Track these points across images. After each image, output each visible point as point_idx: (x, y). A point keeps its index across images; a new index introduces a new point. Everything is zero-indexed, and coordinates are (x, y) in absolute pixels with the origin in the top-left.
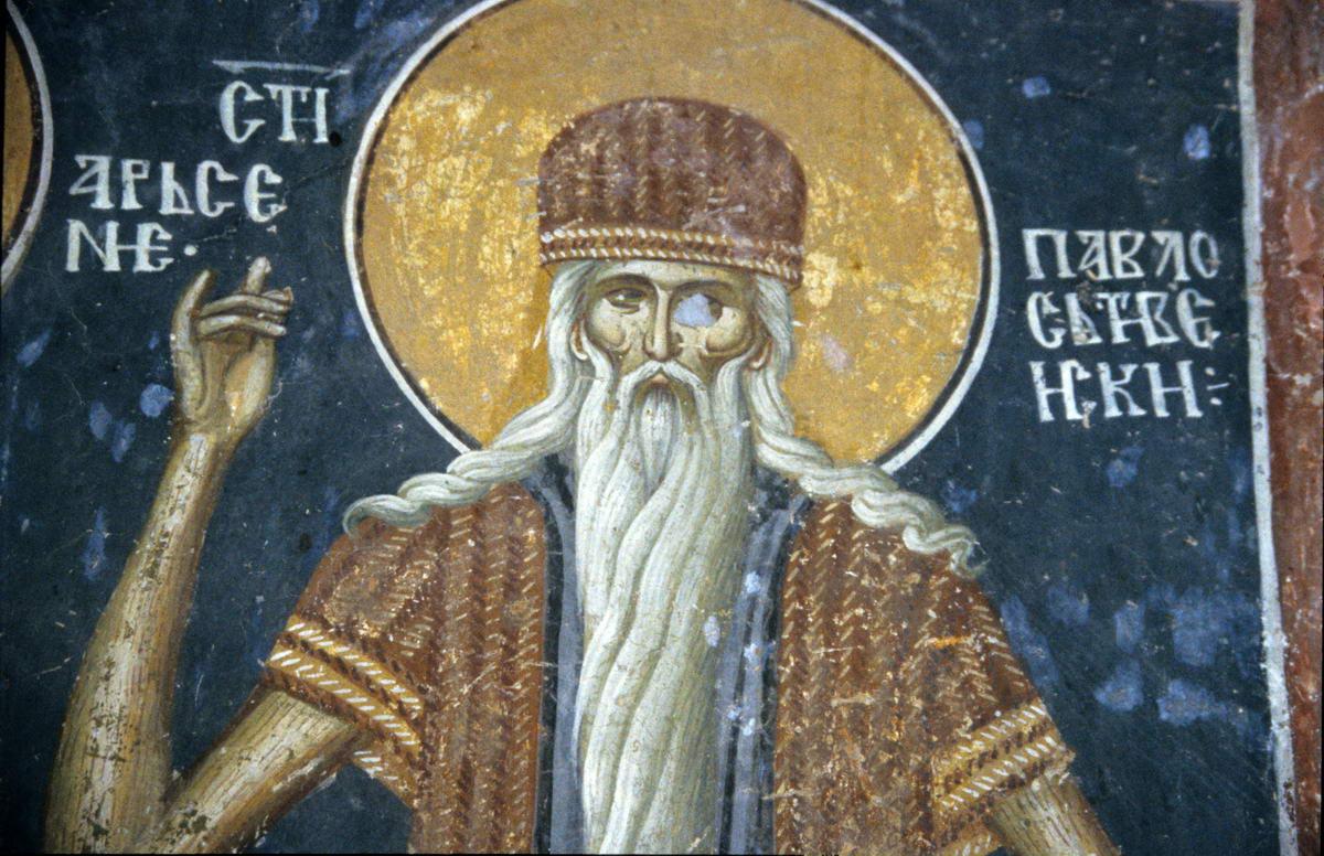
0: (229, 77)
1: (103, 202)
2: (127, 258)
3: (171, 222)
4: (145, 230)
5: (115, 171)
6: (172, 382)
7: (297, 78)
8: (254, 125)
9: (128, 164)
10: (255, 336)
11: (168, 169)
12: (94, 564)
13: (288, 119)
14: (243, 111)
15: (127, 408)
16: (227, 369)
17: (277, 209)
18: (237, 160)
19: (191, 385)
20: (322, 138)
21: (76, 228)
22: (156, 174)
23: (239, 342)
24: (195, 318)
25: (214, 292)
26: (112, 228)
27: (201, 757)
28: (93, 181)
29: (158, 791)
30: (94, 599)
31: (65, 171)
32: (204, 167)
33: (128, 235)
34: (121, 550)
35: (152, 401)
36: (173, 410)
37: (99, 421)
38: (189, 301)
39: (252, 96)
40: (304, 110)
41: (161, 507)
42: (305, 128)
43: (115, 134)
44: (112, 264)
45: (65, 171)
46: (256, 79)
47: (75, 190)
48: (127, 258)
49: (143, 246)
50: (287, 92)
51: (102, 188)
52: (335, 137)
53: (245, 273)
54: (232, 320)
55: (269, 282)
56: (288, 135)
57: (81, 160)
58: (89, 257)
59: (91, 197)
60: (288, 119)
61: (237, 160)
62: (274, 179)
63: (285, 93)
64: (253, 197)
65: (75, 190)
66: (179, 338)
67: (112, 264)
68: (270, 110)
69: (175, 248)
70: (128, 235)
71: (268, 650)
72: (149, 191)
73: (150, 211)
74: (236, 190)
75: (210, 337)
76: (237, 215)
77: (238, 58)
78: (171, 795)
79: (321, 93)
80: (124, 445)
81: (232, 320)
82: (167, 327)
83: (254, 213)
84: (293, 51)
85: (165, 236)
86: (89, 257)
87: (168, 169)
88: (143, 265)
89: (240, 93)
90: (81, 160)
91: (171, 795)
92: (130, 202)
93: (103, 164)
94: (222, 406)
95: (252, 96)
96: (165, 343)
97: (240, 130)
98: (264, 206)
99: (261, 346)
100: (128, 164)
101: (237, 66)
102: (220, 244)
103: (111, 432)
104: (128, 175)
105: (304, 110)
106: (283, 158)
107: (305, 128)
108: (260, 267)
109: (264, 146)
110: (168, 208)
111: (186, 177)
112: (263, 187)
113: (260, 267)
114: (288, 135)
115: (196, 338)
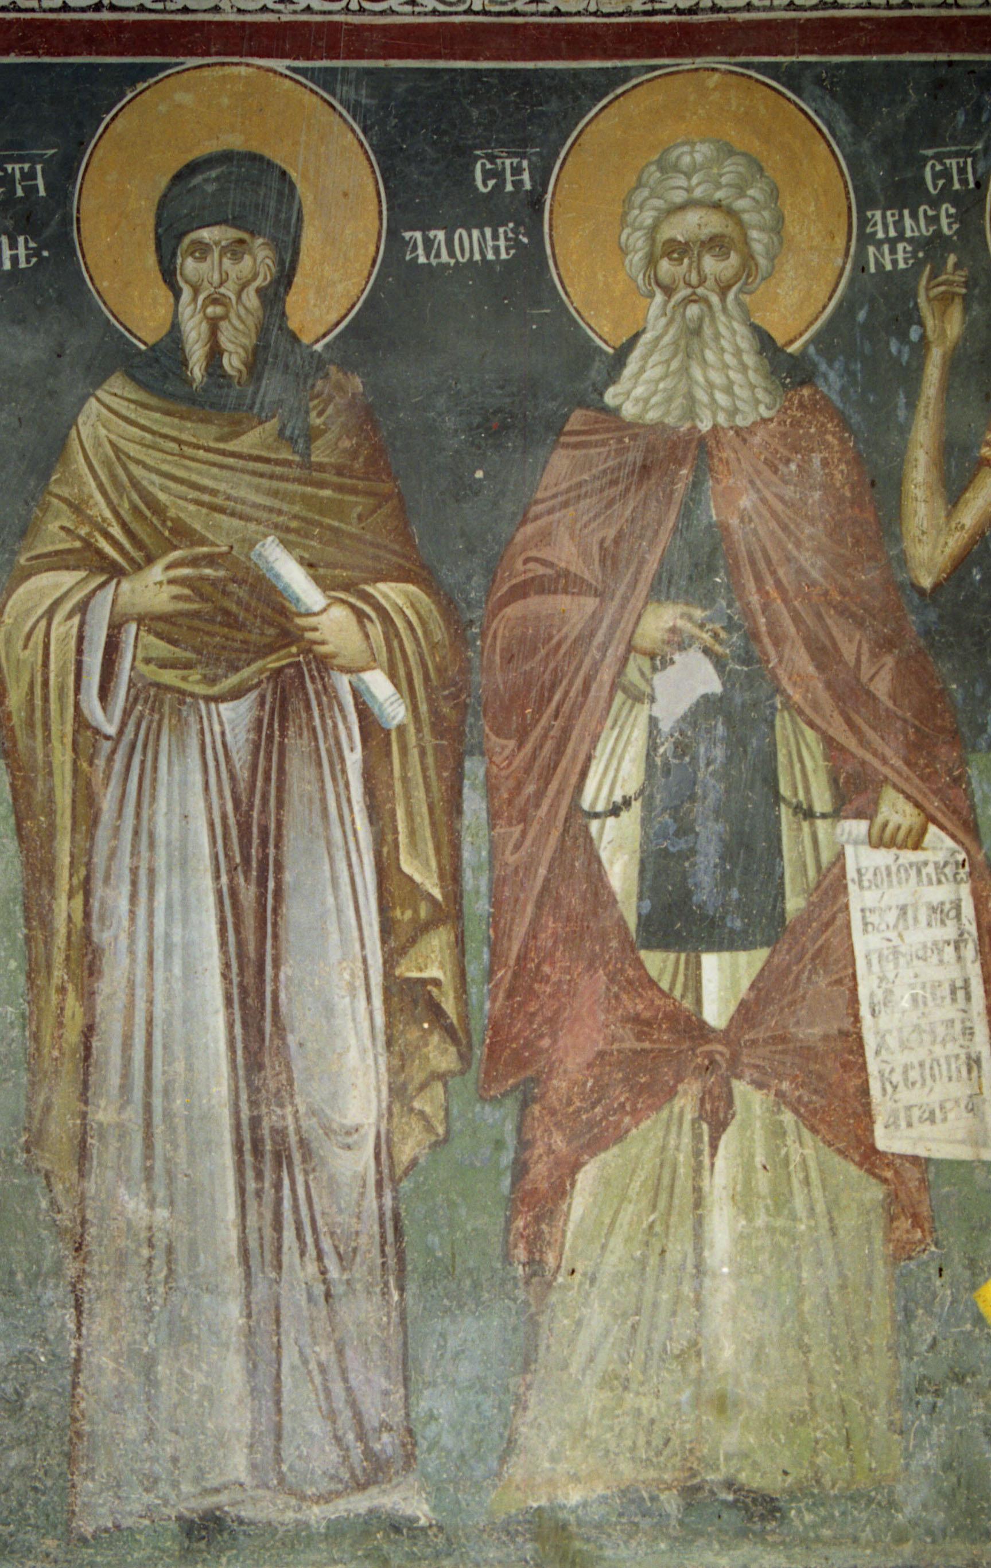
0: (926, 159)
1: (880, 235)
2: (895, 262)
3: (911, 241)
4: (900, 246)
5: (884, 217)
6: (921, 324)
7: (957, 154)
8: (941, 182)
9: (889, 213)
10: (954, 294)
11: (906, 212)
12: (902, 414)
13: (956, 177)
14: (936, 176)
15: (903, 337)
16: (944, 313)
17: (955, 227)
18: (935, 204)
19: (930, 323)
20: (972, 185)
21: (871, 249)
22: (901, 216)
23: (947, 299)
24: (928, 289)
25: (934, 275)
26: (886, 248)
27: (959, 498)
28: (875, 224)
29: (943, 514)
30: (905, 430)
31: (864, 221)
32: (921, 209)
33: (893, 251)
34: (912, 405)
35: (914, 333)
36: (923, 337)
37: (894, 348)
38: (923, 282)
39: (938, 168)
40: (962, 171)
41: (926, 385)
42: (964, 182)
43: (882, 198)
44: (889, 267)
45: (864, 221)
46: (939, 157)
47: (869, 230)
48: (895, 262)
49: (900, 256)
50: (954, 162)
51: (879, 227)
52: (978, 185)
53: (945, 263)
54: (942, 288)
55: (957, 266)
56: (957, 186)
57: (869, 214)
58: (879, 265)
59: (875, 233)
60: (956, 177)
61: (935, 204)
62: (952, 211)
63: (952, 163)
64: (944, 221)
65: (869, 230)
66: (922, 300)
67: (889, 267)
68: (946, 174)
69: (914, 254)
70: (893, 251)
71: (979, 448)
72: (899, 224)
73: (901, 237)
74: (934, 220)
75: (935, 298)
76: (938, 233)
77: (930, 147)
78: (949, 516)
79: (969, 160)
80: (905, 357)
81: (942, 288)
82: (915, 296)
83: (946, 230)
84: (954, 140)
85: (909, 248)
86: (879, 265)
87: (906, 212)
88: (902, 265)
89: (933, 167)
90: (869, 214)
91: (949, 516)
92: (892, 233)
93: (878, 214)
94: (943, 331)
95: (938, 168)
96: (916, 304)
97: (935, 186)
98: (950, 225)
99: (958, 301)
100: (889, 213)
101: (930, 152)
102: (932, 248)
103: (900, 352)
104: (890, 220)
105: (962, 171)
106: (956, 199)
107: (964, 182)
108: (952, 259)
109: (946, 194)
110: (909, 234)
111: (914, 216)
112: (948, 216)
113: (952, 259)
114: (957, 186)
115: (929, 300)
